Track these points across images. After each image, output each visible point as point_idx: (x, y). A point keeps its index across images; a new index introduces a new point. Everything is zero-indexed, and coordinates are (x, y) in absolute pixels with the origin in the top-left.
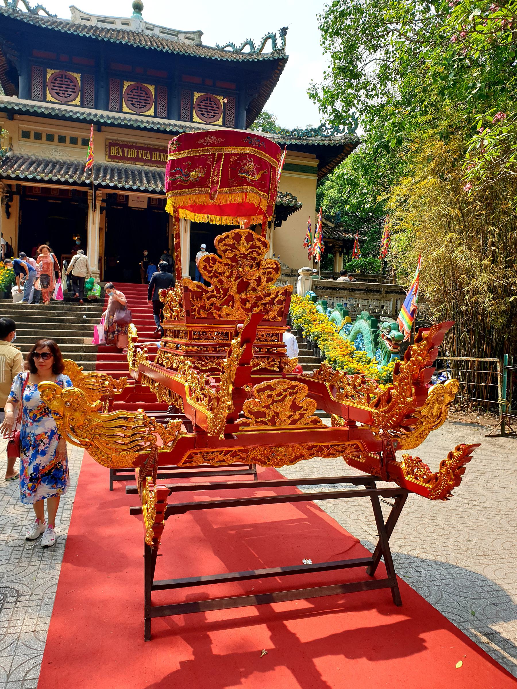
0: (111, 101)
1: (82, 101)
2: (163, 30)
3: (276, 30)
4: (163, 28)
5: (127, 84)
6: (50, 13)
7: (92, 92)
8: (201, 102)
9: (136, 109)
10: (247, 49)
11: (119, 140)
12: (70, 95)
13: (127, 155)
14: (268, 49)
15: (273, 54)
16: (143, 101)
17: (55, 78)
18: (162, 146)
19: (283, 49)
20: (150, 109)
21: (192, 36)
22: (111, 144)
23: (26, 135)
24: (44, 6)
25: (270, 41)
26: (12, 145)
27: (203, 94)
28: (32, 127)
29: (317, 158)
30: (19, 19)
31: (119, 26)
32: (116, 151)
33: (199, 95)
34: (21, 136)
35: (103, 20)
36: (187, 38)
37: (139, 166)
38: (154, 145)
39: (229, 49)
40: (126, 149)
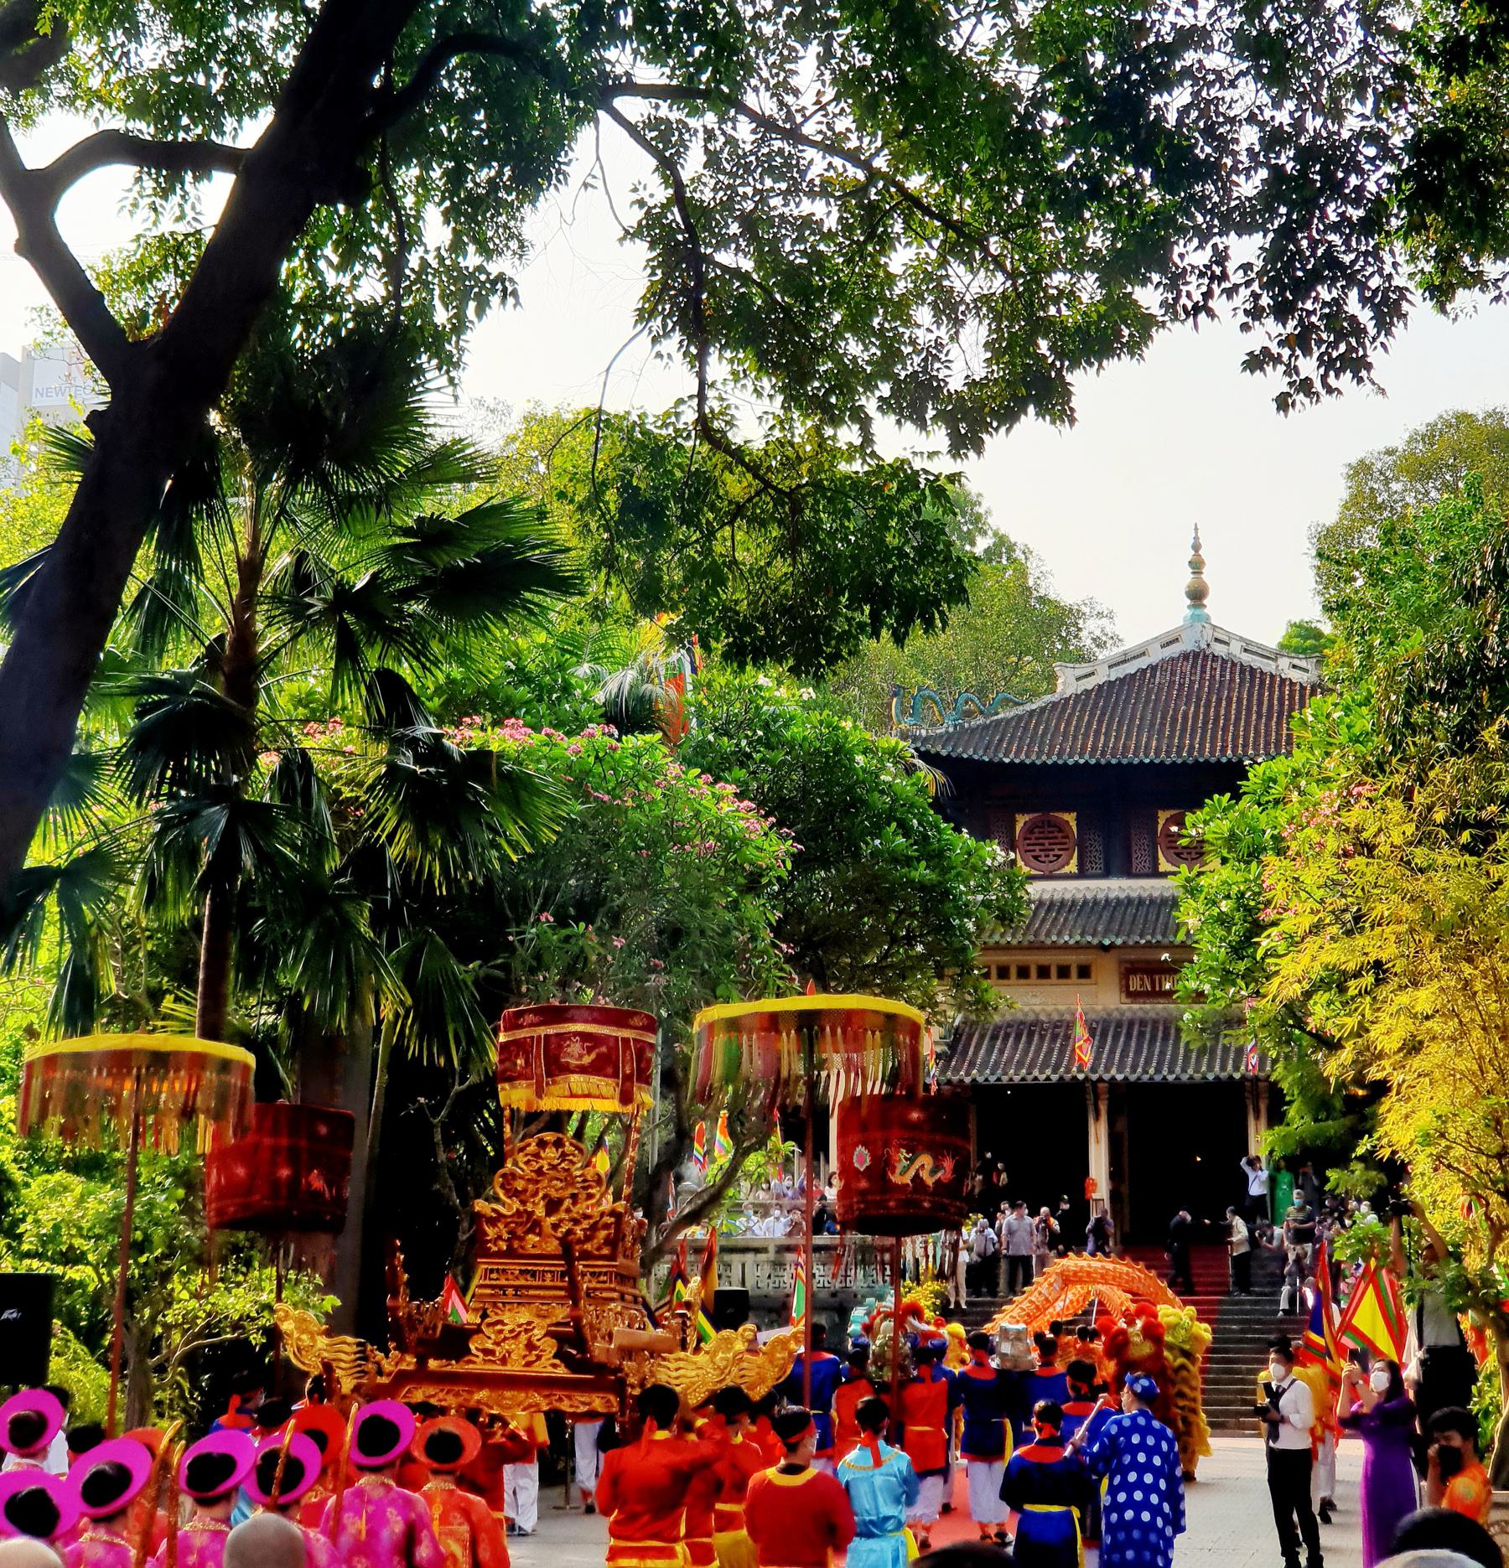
1: (1081, 865)
4: (1249, 642)
17: (1029, 829)
22: (1129, 970)
31: (1156, 656)
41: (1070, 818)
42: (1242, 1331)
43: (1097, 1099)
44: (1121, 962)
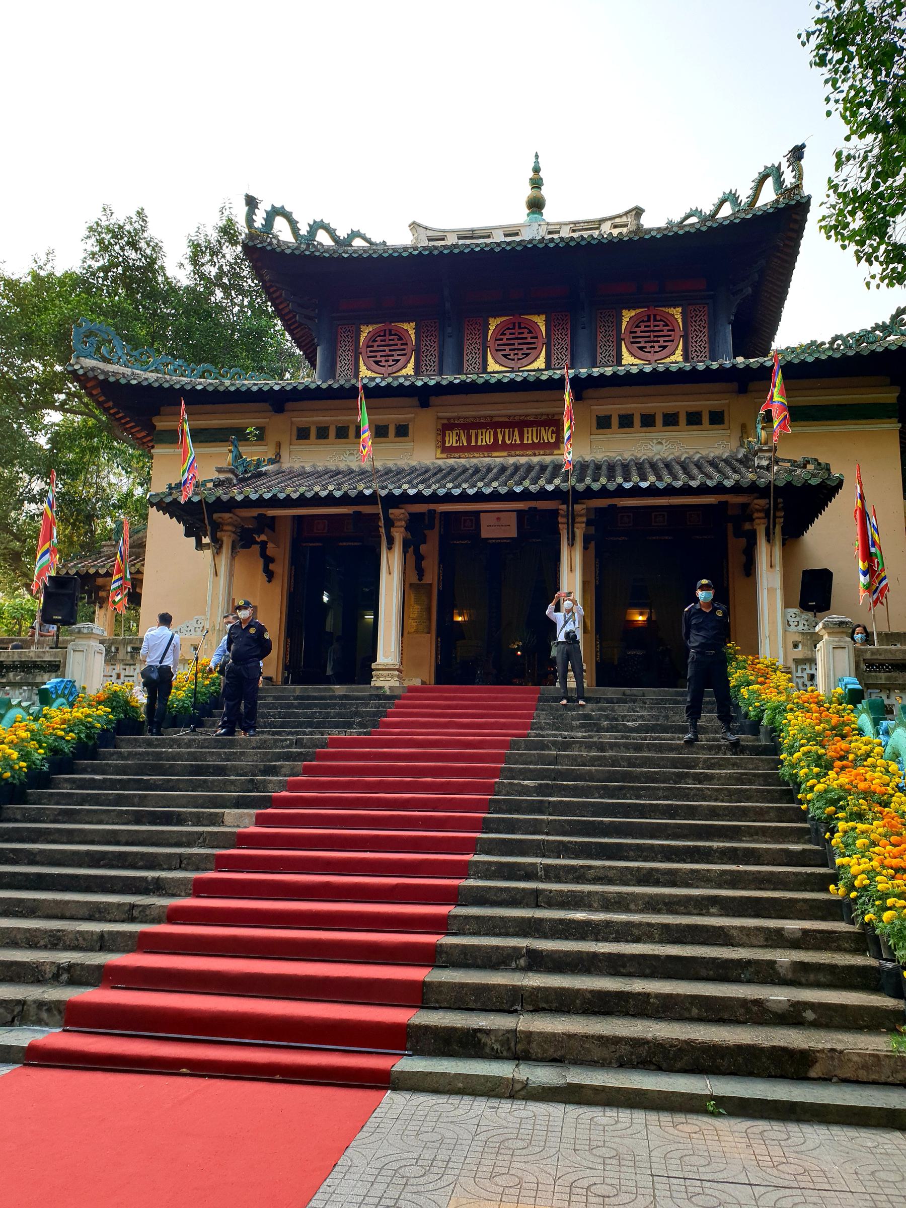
0: (466, 358)
2: (575, 226)
3: (778, 156)
4: (575, 223)
5: (493, 324)
6: (373, 240)
7: (432, 351)
8: (637, 326)
9: (512, 364)
10: (727, 211)
11: (459, 418)
12: (398, 361)
13: (476, 441)
14: (768, 195)
15: (777, 201)
16: (525, 347)
17: (372, 338)
18: (542, 415)
19: (798, 187)
20: (538, 357)
21: (624, 219)
23: (303, 434)
24: (362, 232)
25: (769, 182)
26: (278, 455)
27: (638, 311)
28: (312, 419)
29: (892, 384)
30: (307, 253)
32: (455, 438)
33: (633, 313)
34: (294, 437)
35: (472, 234)
36: (615, 227)
37: (498, 459)
38: (527, 416)
39: (693, 220)
40: (473, 432)
41: (410, 328)
42: (541, 790)
43: (389, 524)
44: (438, 418)
